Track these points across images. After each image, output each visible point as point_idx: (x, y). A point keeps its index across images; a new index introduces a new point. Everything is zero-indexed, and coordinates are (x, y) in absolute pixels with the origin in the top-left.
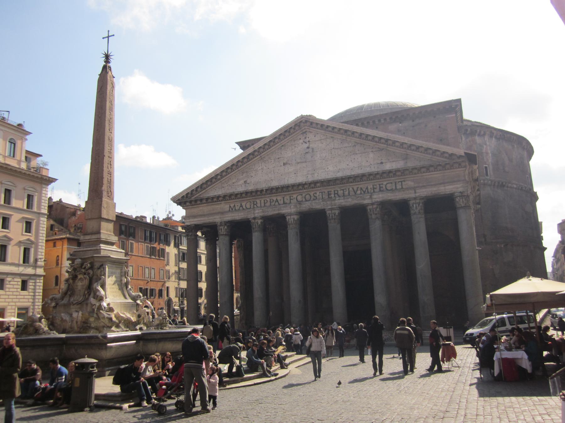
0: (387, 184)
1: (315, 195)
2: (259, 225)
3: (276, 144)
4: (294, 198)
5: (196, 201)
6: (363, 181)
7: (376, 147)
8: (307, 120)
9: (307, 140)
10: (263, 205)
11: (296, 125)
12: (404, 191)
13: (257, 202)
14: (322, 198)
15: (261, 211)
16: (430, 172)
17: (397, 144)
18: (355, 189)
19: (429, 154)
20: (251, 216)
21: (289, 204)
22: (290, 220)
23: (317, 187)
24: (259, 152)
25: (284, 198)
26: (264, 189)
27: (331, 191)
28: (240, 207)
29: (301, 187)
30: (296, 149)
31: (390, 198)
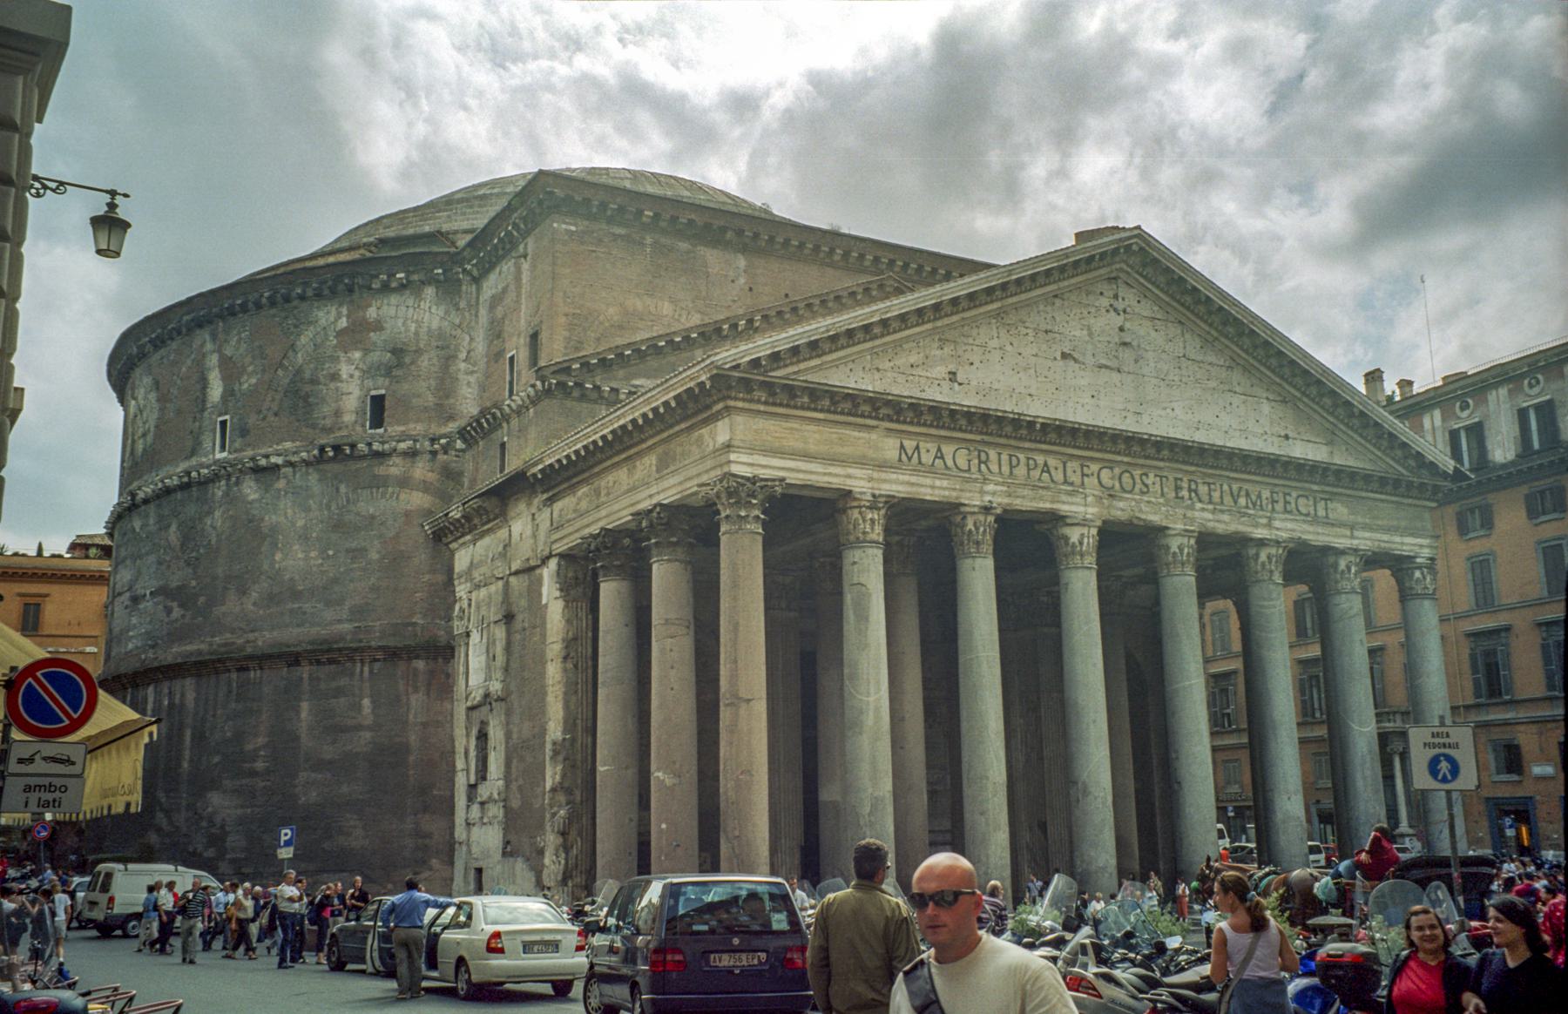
0: (1299, 497)
6: (1259, 474)
9: (1120, 305)
10: (1006, 469)
12: (1333, 525)
14: (1163, 495)
15: (1005, 489)
16: (1381, 493)
18: (1235, 487)
19: (1379, 449)
20: (973, 499)
22: (1086, 540)
23: (1157, 459)
25: (1064, 464)
26: (1040, 420)
28: (936, 457)
30: (1092, 321)
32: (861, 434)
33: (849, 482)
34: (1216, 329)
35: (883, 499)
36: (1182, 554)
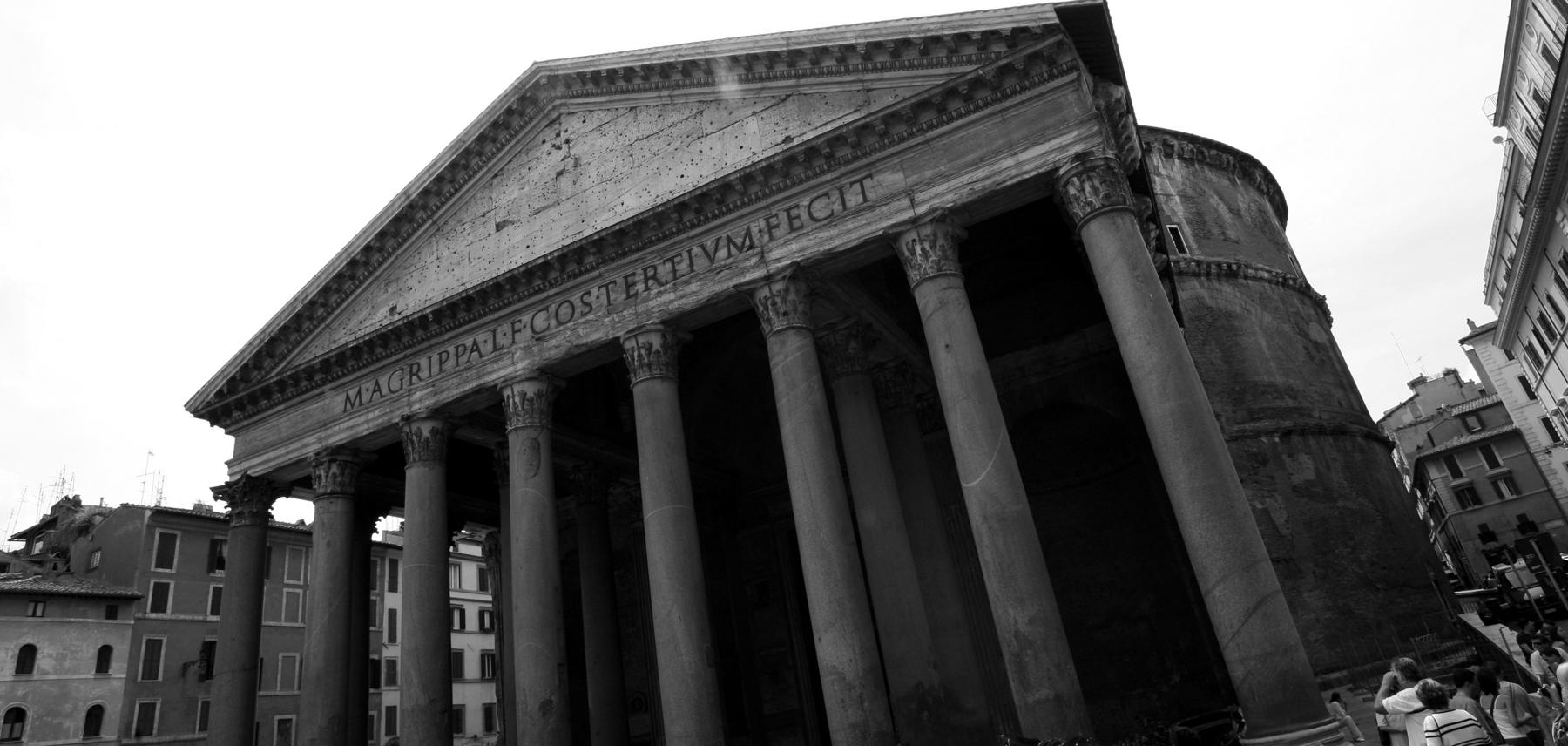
0: (813, 200)
1: (586, 298)
2: (427, 440)
3: (475, 173)
4: (525, 327)
5: (253, 399)
6: (729, 211)
7: (765, 97)
8: (552, 74)
10: (435, 369)
11: (522, 99)
12: (871, 208)
13: (418, 364)
15: (431, 389)
16: (951, 120)
17: (829, 63)
18: (710, 244)
19: (940, 65)
21: (508, 348)
22: (511, 401)
23: (587, 271)
24: (425, 207)
26: (428, 311)
27: (634, 274)
28: (374, 391)
29: (538, 282)
31: (827, 247)
32: (319, 404)
33: (305, 451)
34: (664, 87)
35: (324, 453)
36: (634, 359)
